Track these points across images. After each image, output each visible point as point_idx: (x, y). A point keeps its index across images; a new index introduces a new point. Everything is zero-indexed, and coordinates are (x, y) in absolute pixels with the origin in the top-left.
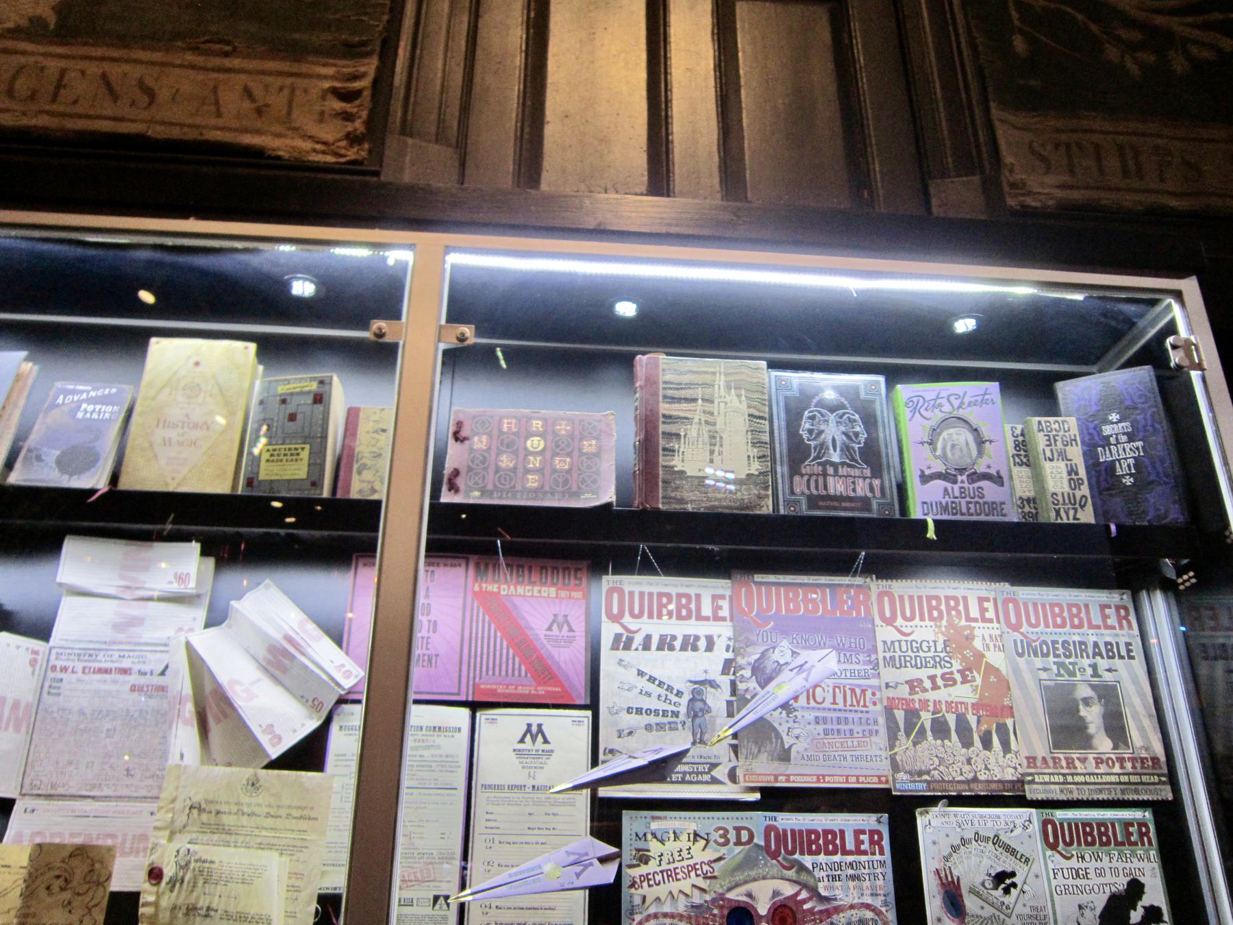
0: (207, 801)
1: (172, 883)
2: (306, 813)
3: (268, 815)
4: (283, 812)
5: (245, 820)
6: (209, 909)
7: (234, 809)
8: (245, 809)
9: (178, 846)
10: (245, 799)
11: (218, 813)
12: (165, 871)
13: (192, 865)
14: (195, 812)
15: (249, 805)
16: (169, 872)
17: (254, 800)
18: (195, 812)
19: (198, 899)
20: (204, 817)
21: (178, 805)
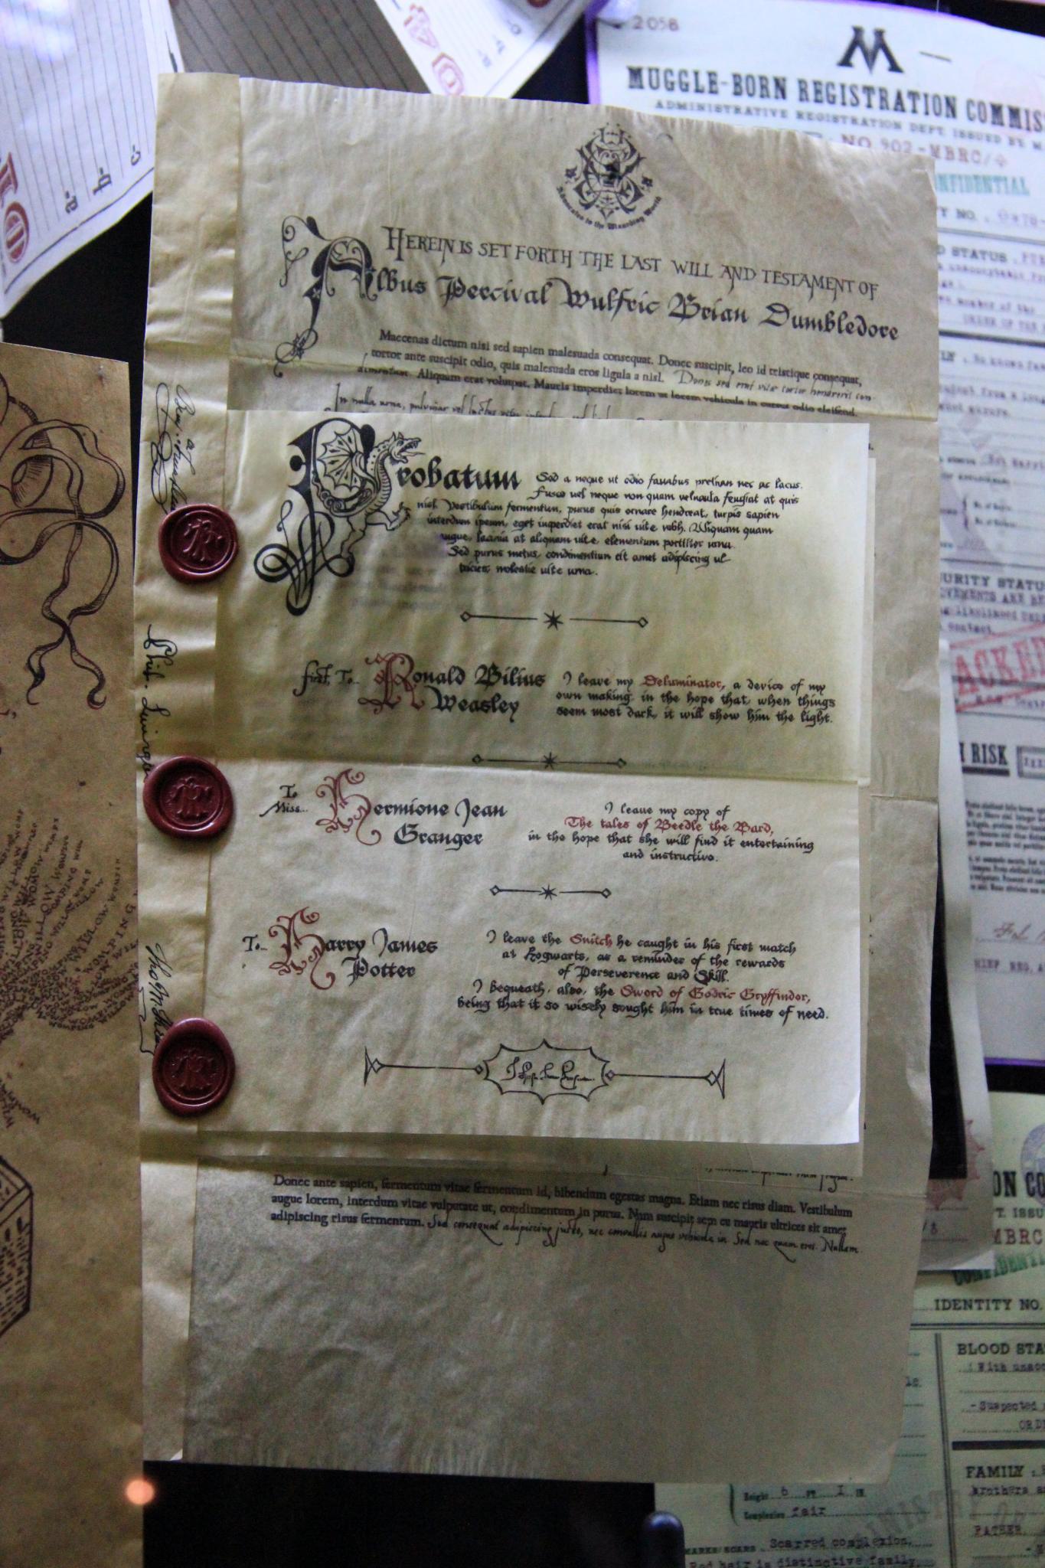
0: (397, 237)
1: (295, 573)
2: (851, 303)
3: (686, 308)
4: (752, 297)
5: (581, 328)
6: (492, 674)
7: (530, 276)
8: (582, 281)
9: (304, 419)
10: (574, 235)
11: (454, 290)
12: (247, 525)
13: (397, 495)
14: (346, 283)
15: (601, 261)
16: (267, 522)
17: (622, 241)
18: (346, 283)
19: (433, 636)
20: (392, 308)
21: (257, 251)
